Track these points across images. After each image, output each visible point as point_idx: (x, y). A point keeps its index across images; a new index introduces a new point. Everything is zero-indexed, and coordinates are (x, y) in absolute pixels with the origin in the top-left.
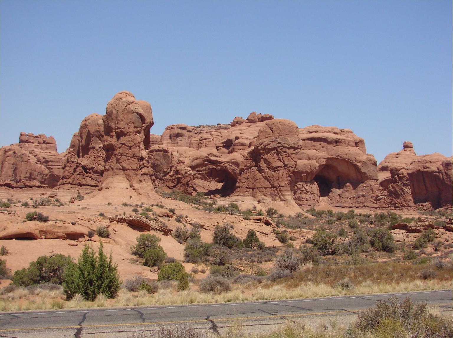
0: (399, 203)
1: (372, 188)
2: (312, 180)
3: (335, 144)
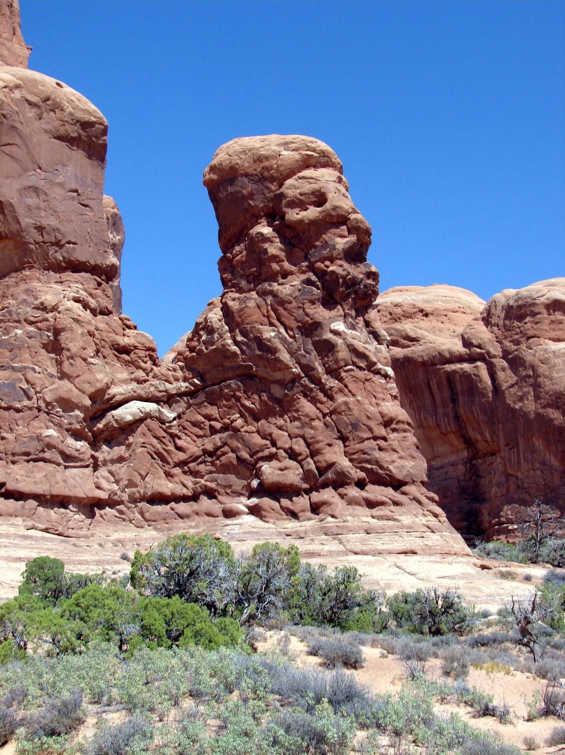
0: (293, 455)
1: (57, 332)
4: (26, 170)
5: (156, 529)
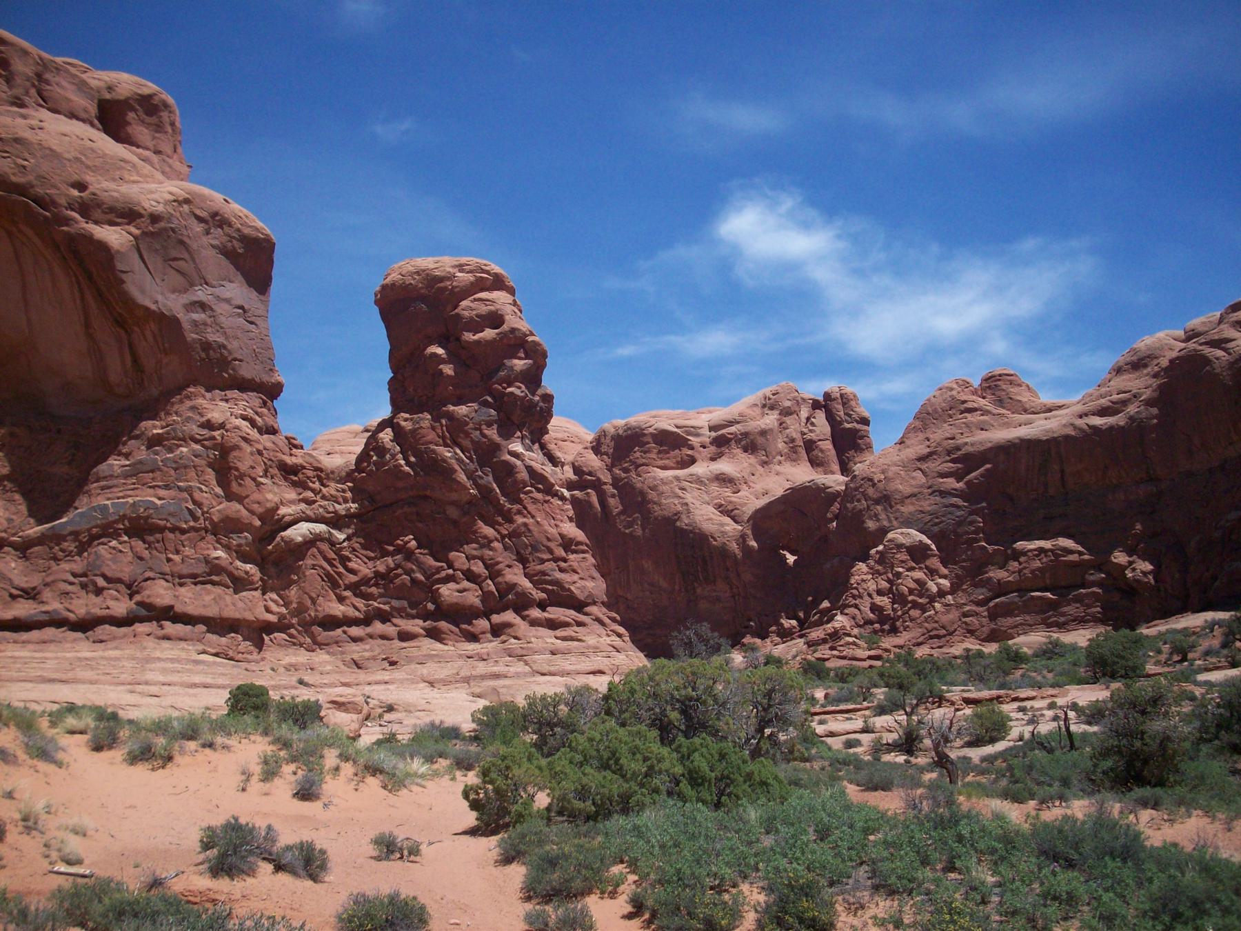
0: (471, 576)
4: (192, 285)
5: (328, 653)
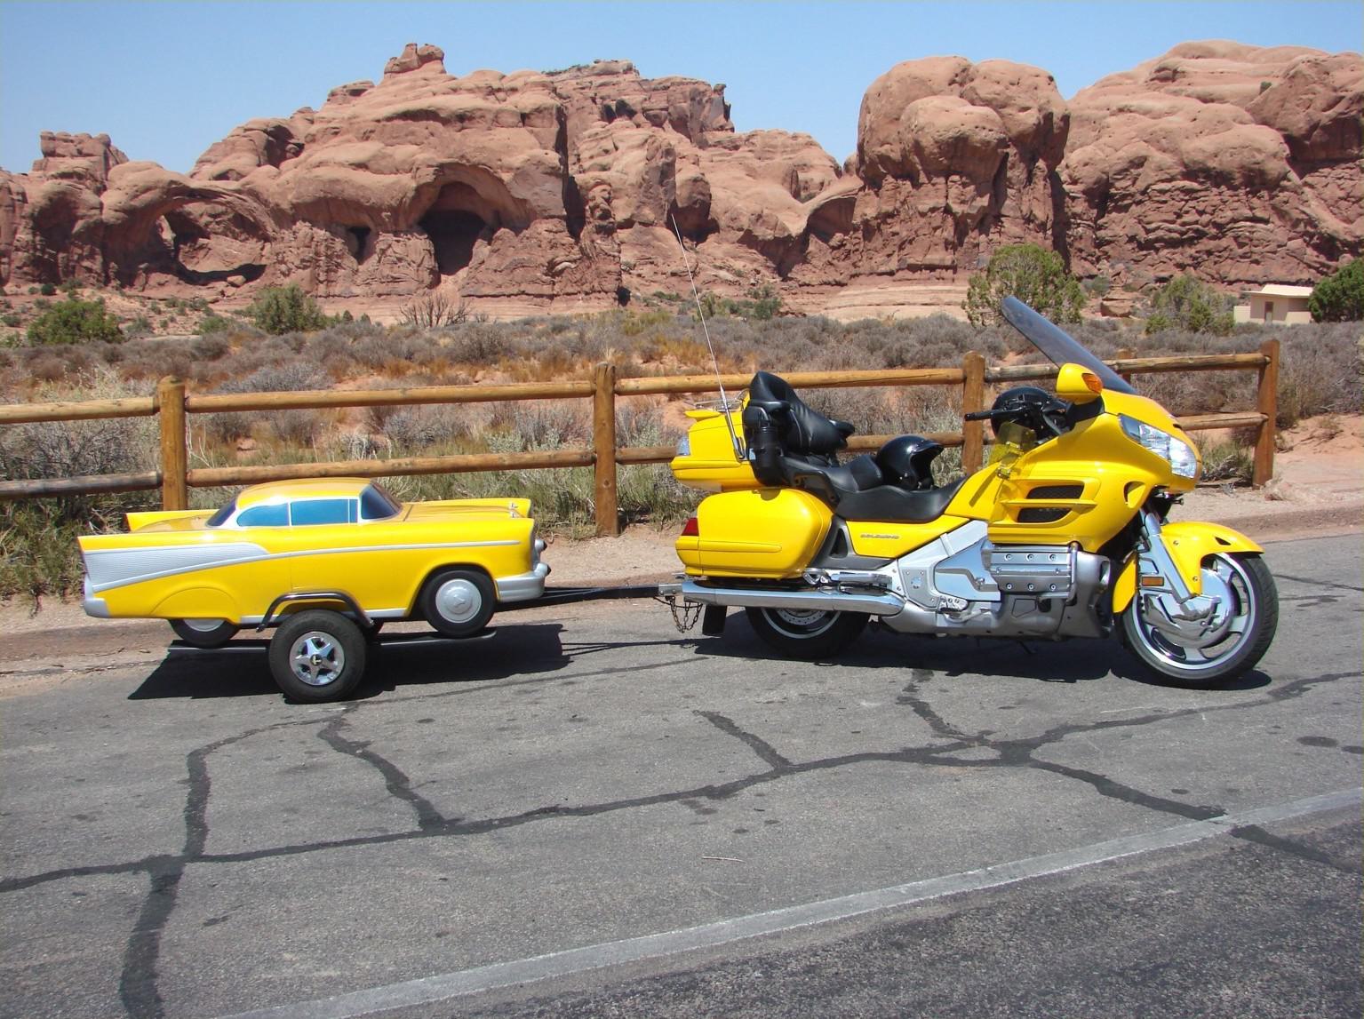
2: (411, 227)
3: (459, 125)
